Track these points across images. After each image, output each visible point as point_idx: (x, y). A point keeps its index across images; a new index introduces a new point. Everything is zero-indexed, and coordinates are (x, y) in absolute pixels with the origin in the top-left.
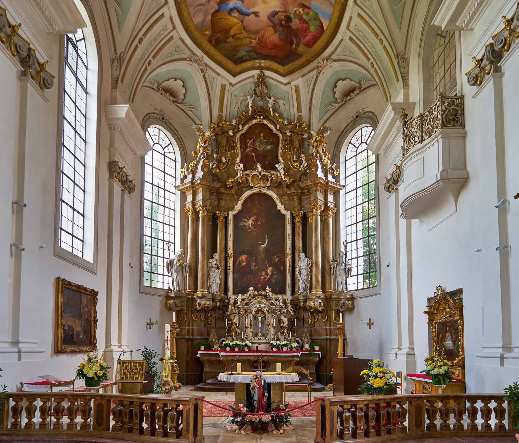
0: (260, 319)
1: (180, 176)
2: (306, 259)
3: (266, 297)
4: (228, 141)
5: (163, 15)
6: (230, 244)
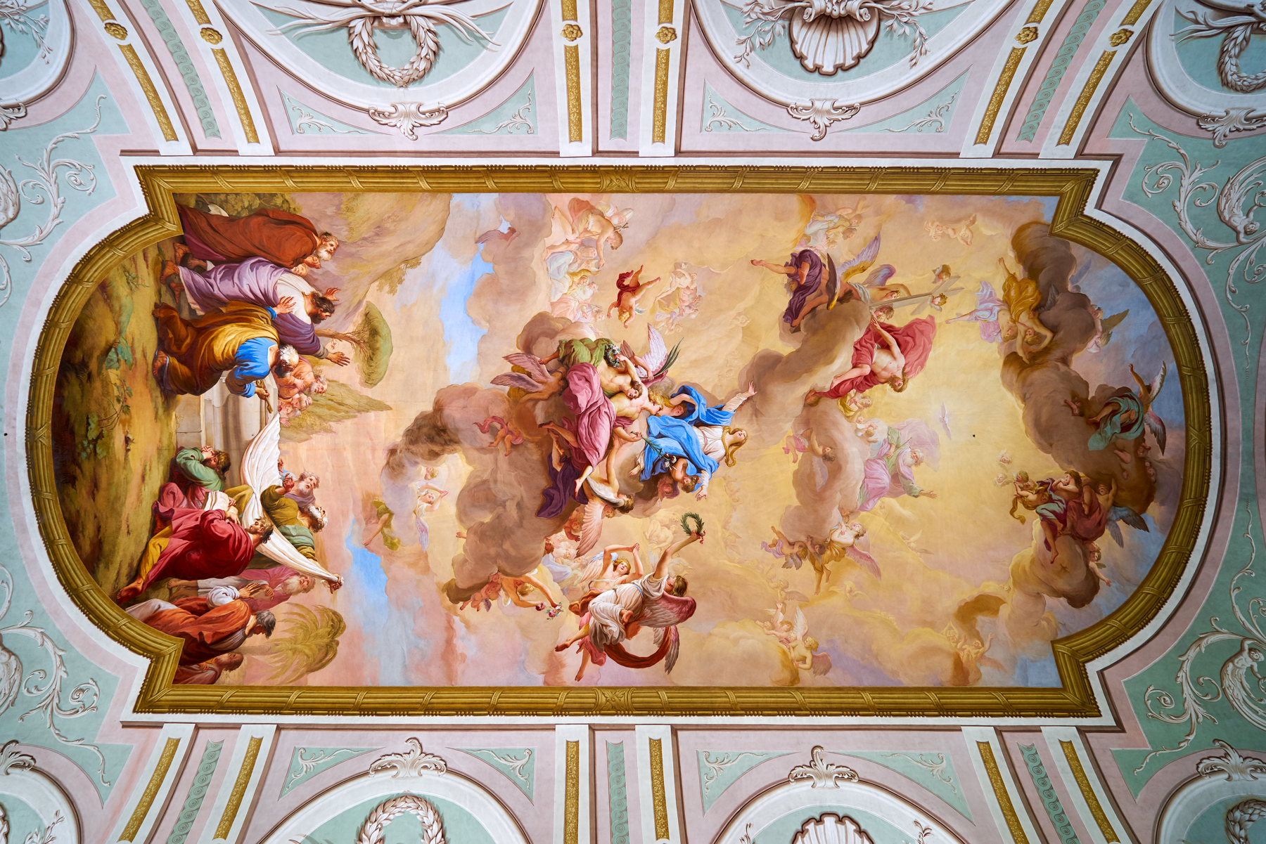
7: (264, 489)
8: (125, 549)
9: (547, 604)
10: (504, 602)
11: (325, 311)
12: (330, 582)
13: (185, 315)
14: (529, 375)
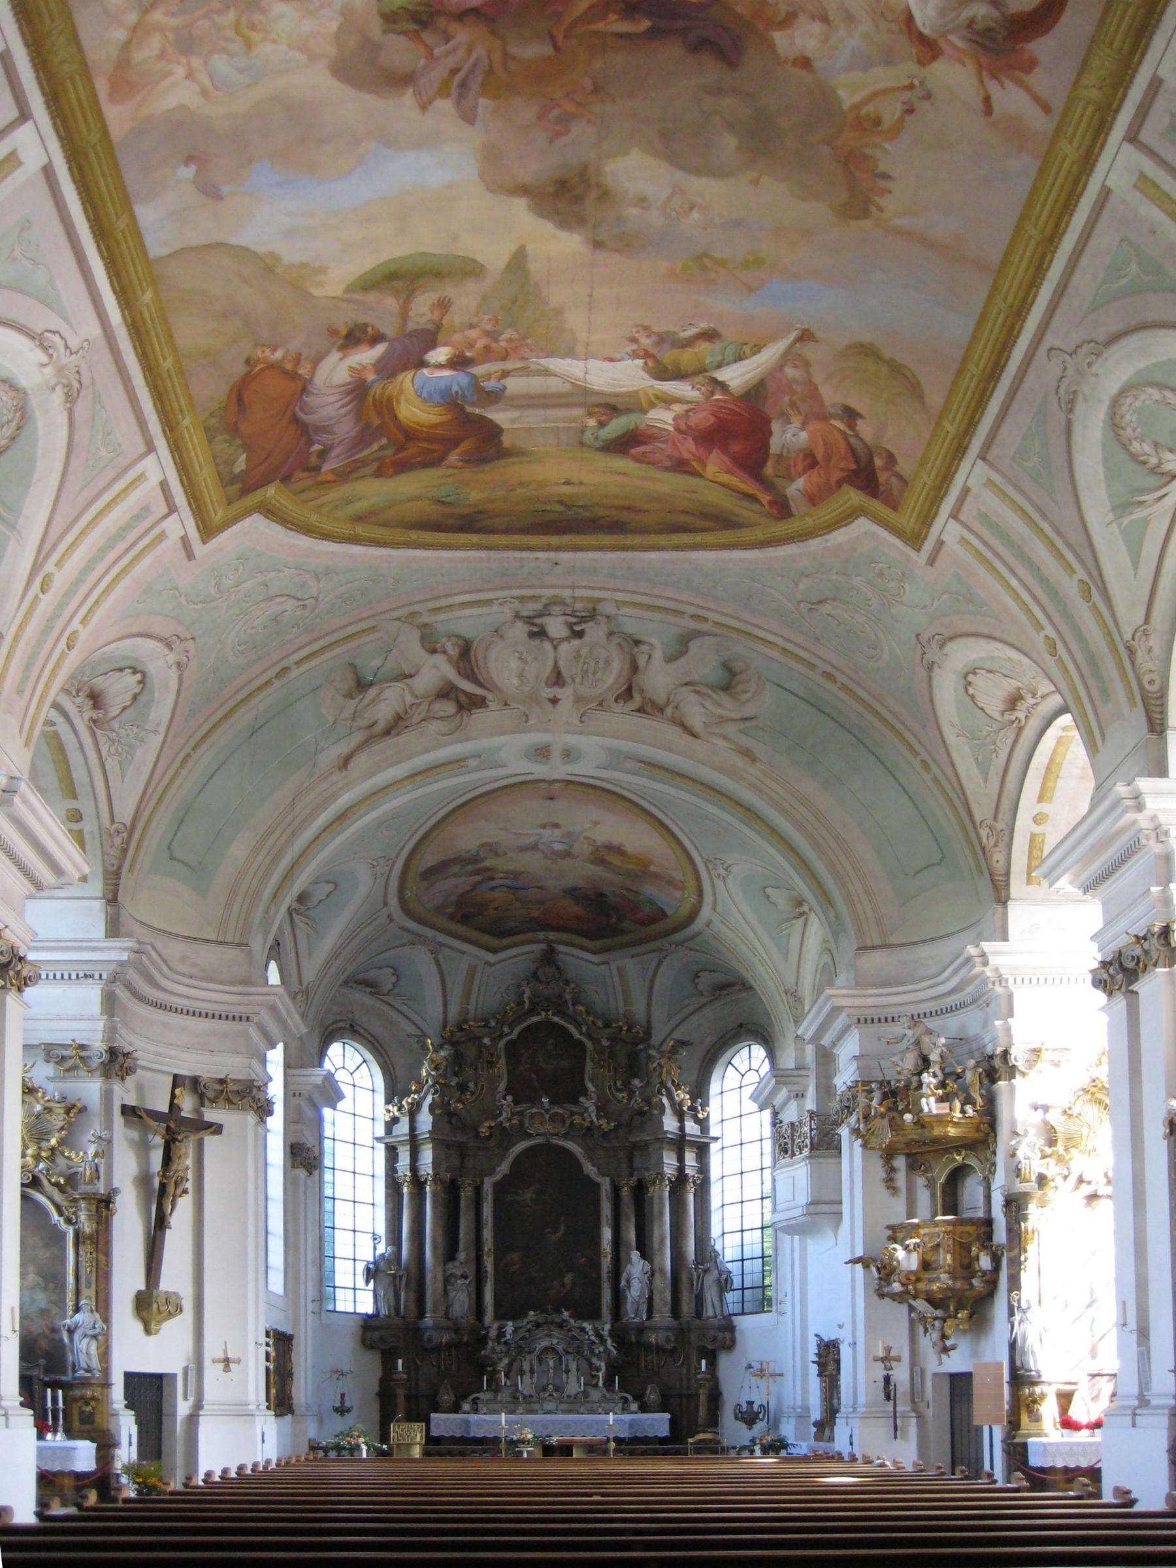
0: (551, 1363)
1: (382, 1116)
2: (642, 1262)
3: (561, 1325)
4: (480, 1055)
5: (141, 477)
6: (488, 1234)
7: (646, 375)
8: (715, 497)
9: (906, 96)
10: (889, 156)
11: (365, 332)
12: (801, 339)
13: (388, 452)
14: (454, 72)
